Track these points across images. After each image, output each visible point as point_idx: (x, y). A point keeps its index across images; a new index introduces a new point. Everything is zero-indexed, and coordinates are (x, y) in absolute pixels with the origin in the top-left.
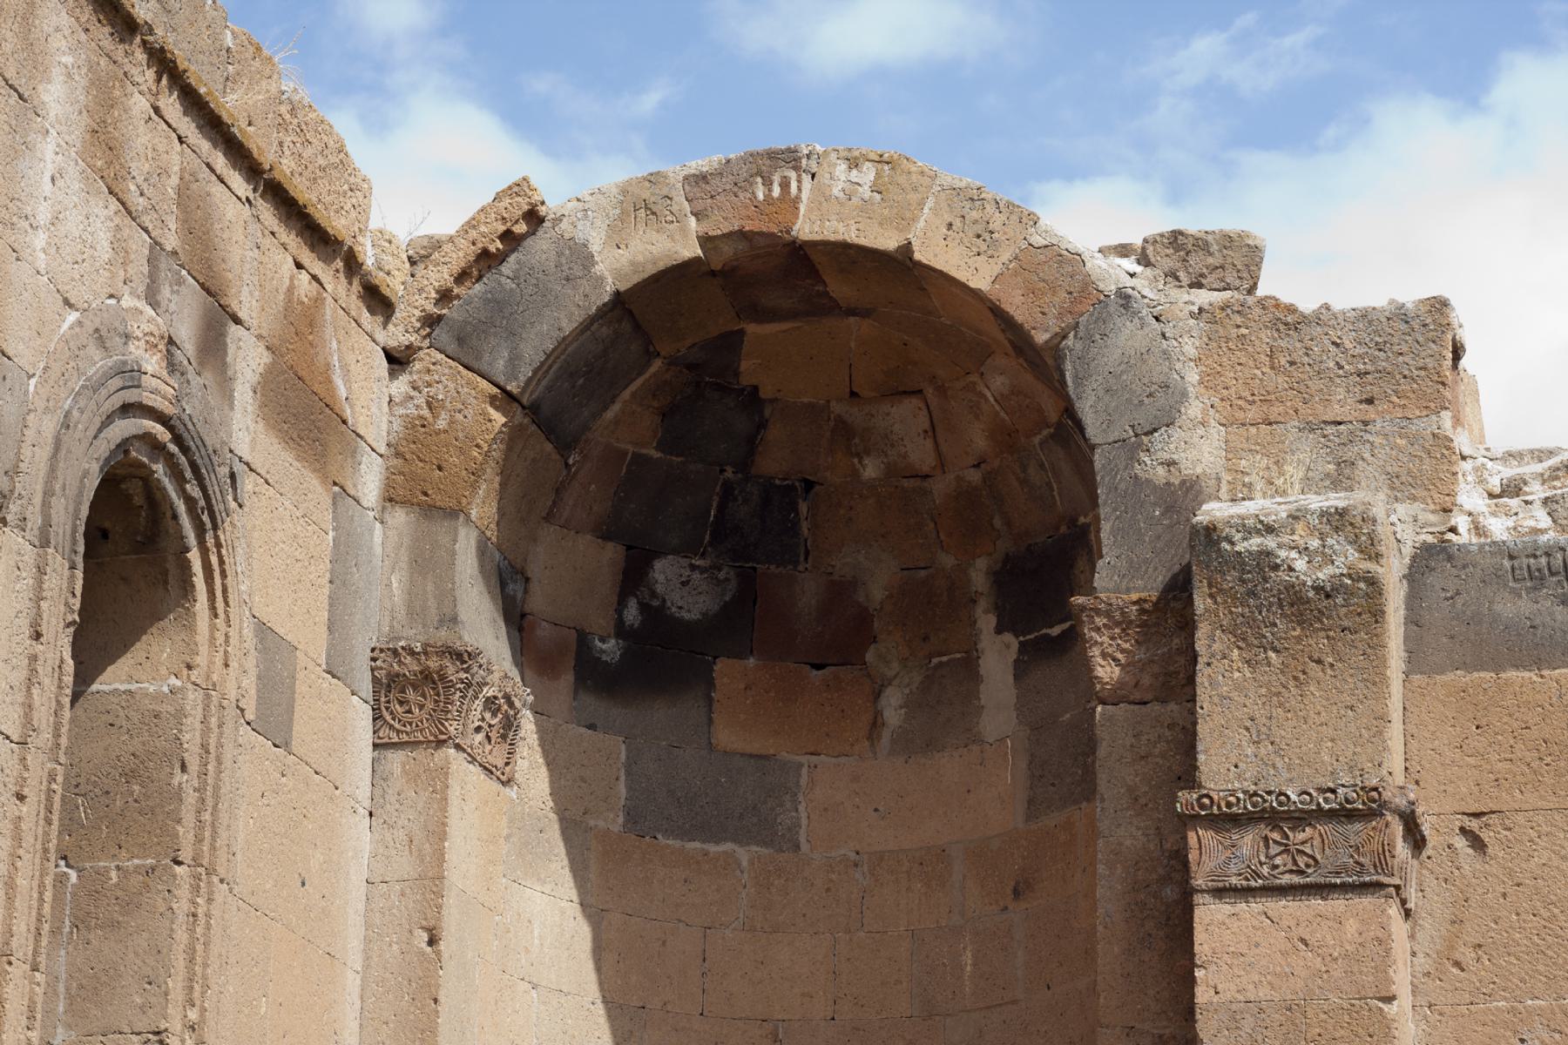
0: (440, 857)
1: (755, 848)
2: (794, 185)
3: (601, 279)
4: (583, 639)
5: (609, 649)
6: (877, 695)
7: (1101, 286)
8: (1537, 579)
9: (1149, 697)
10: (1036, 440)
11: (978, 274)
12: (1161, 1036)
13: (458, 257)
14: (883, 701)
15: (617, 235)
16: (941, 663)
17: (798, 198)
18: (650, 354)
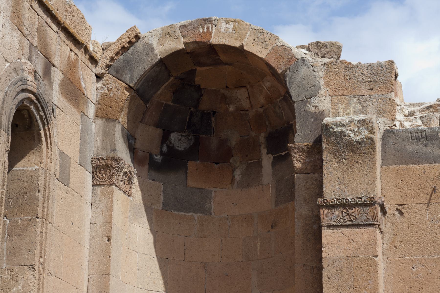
0: (111, 216)
1: (199, 214)
3: (156, 55)
4: (151, 155)
5: (158, 158)
6: (233, 171)
7: (297, 57)
8: (418, 139)
9: (309, 172)
10: (278, 100)
11: (262, 53)
12: (312, 267)
13: (116, 48)
14: (235, 173)
15: (161, 42)
16: (251, 163)
17: (212, 32)
18: (170, 76)
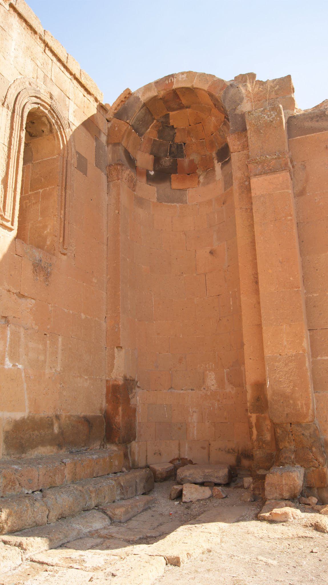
1: (180, 204)
2: (173, 80)
3: (141, 101)
4: (147, 171)
5: (152, 173)
6: (199, 177)
7: (227, 84)
8: (312, 119)
9: (240, 150)
10: (221, 126)
12: (247, 209)
14: (200, 179)
16: (209, 171)
17: (174, 82)
18: (154, 119)
